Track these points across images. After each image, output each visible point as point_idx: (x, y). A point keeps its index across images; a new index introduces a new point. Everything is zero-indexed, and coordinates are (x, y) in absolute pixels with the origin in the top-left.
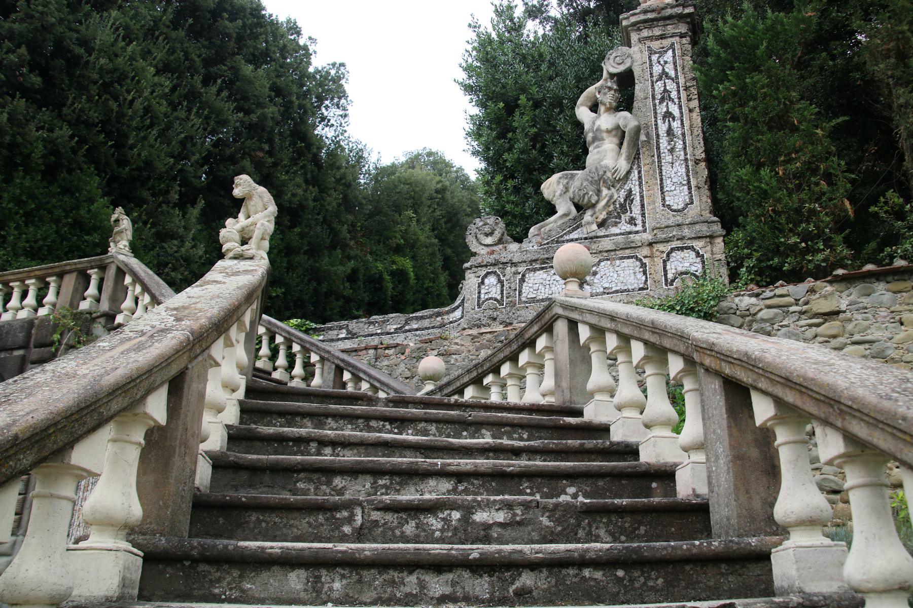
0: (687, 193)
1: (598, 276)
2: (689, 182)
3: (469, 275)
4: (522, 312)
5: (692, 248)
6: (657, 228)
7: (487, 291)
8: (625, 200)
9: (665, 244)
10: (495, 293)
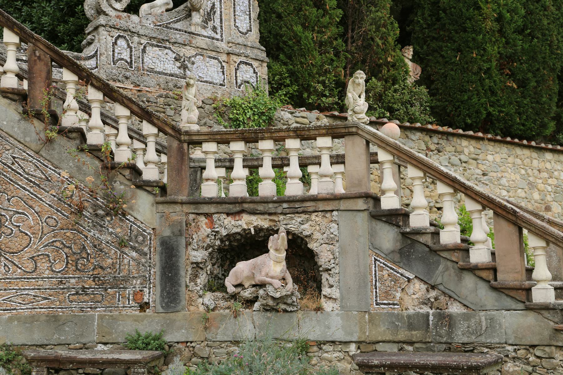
0: (248, 22)
1: (195, 66)
2: (250, 14)
3: (101, 29)
4: (145, 78)
5: (251, 65)
6: (232, 43)
7: (119, 52)
8: (211, 11)
9: (237, 57)
10: (126, 55)
